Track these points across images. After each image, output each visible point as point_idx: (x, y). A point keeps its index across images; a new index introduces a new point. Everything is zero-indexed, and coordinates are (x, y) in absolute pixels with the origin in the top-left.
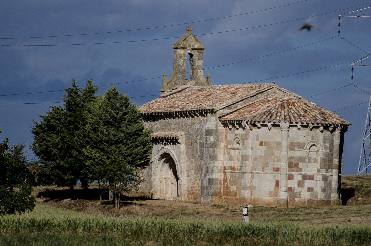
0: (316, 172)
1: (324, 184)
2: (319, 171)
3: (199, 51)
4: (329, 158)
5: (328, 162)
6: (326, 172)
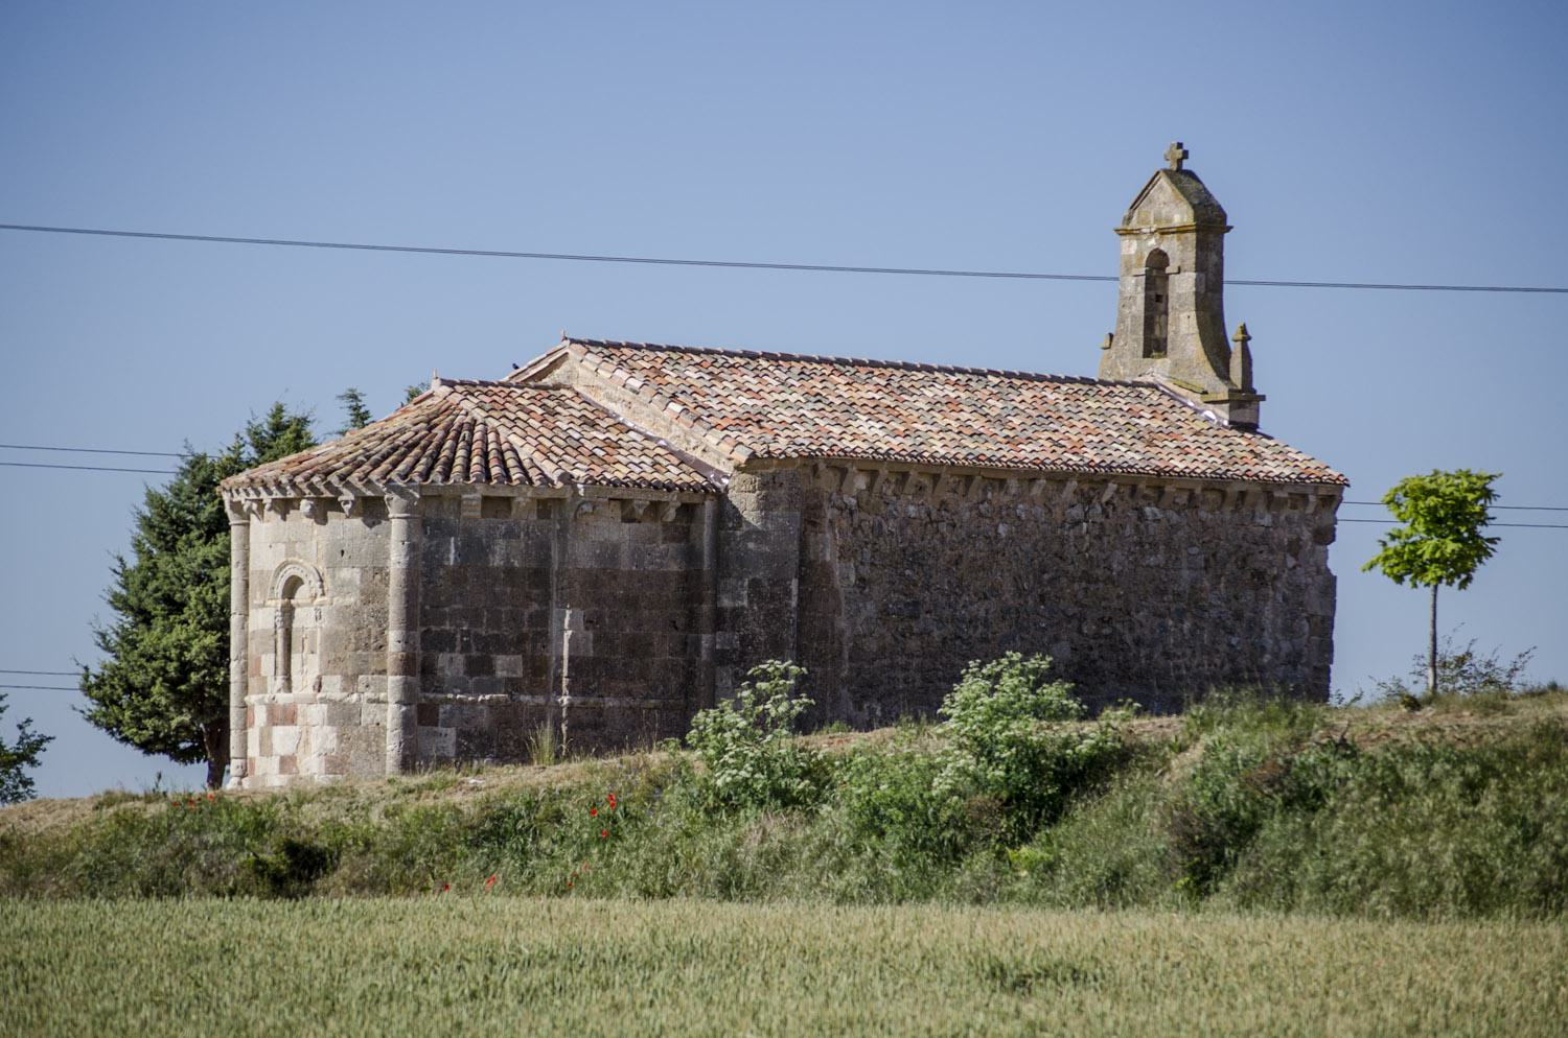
0: (310, 691)
2: (319, 687)
5: (352, 646)
6: (344, 690)
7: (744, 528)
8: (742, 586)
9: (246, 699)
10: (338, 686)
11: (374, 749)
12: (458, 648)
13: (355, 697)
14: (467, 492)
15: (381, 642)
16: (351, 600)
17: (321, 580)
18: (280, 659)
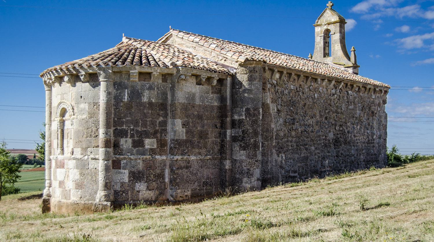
0: (69, 155)
1: (81, 174)
2: (73, 153)
3: (335, 24)
4: (88, 129)
5: (85, 136)
6: (82, 154)
7: (243, 88)
8: (243, 111)
9: (50, 157)
10: (80, 153)
11: (94, 179)
12: (129, 136)
13: (86, 157)
14: (132, 70)
15: (97, 134)
16: (84, 116)
17: (73, 109)
18: (59, 142)
